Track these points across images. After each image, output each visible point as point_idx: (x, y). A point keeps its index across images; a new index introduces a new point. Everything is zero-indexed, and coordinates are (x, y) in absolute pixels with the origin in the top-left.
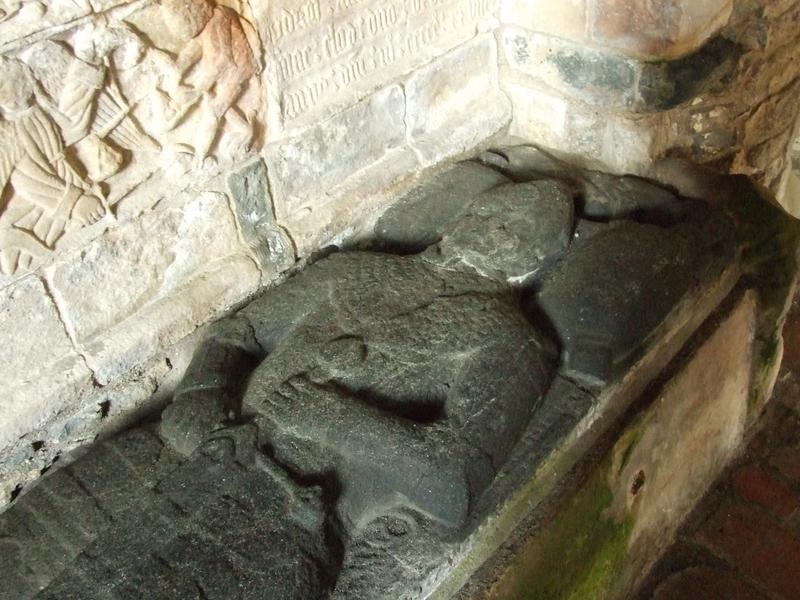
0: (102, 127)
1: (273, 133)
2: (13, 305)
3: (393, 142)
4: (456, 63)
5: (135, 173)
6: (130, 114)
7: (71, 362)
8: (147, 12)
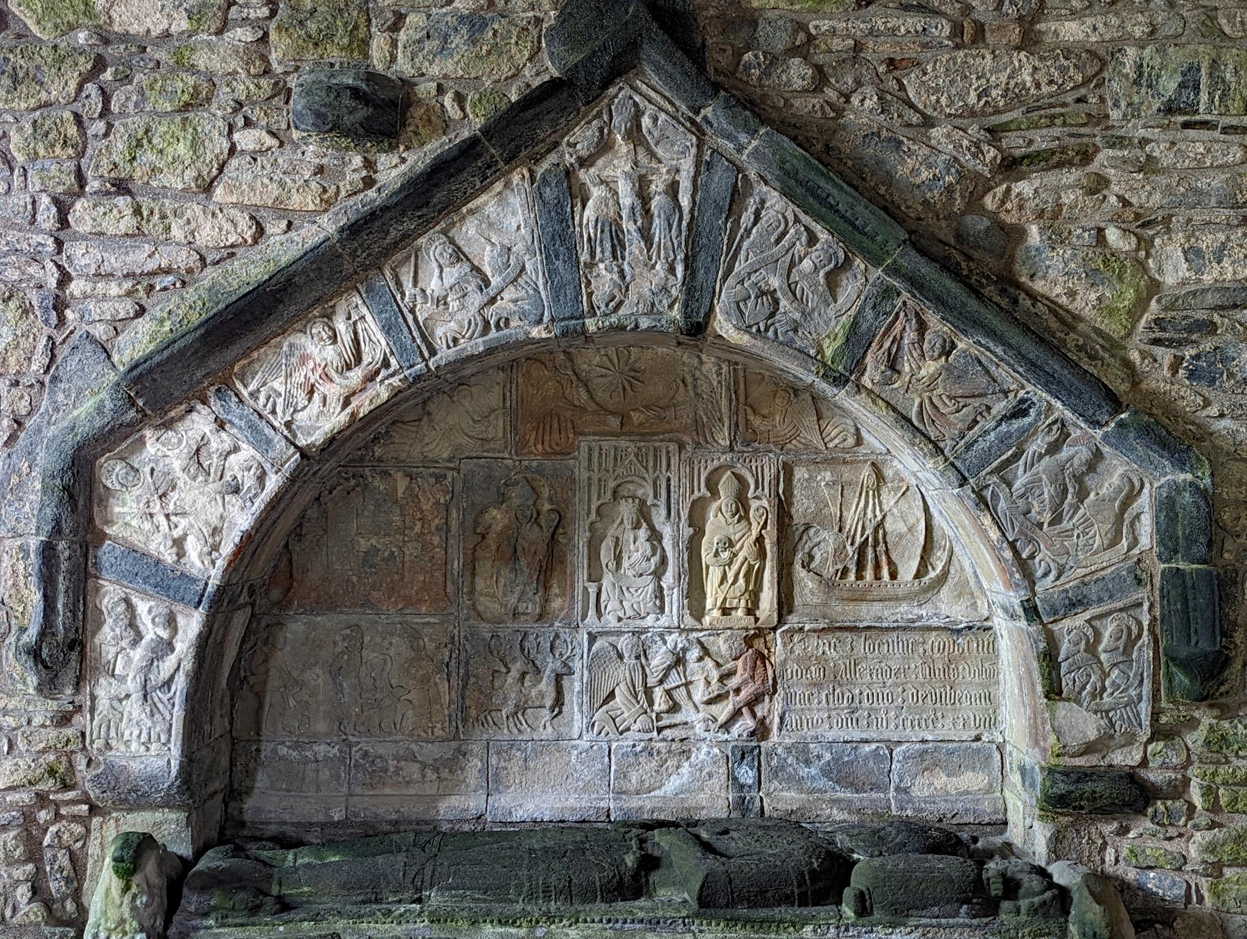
0: (667, 686)
1: (774, 737)
2: (590, 753)
3: (876, 787)
4: (950, 753)
5: (678, 718)
6: (687, 684)
7: (602, 799)
8: (712, 638)
